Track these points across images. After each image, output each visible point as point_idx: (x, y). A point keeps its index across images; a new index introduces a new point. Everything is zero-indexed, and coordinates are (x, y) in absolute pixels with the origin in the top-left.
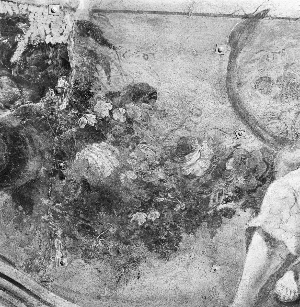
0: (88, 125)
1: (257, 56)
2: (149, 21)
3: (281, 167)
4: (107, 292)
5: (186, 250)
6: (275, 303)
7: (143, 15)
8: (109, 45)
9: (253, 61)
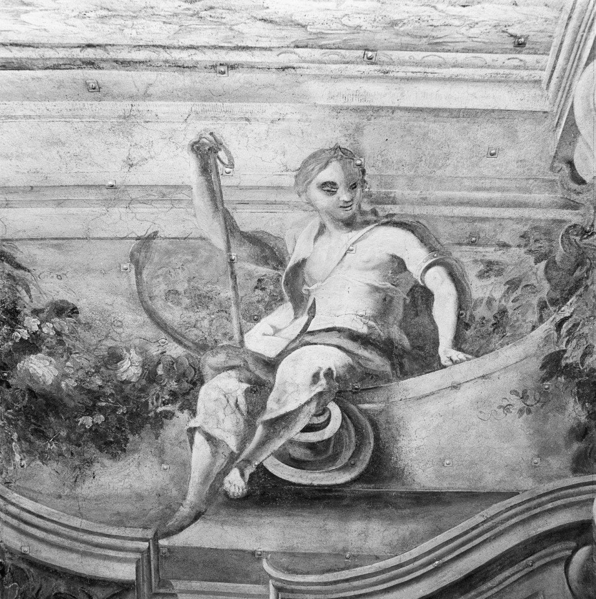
0: (22, 339)
1: (160, 272)
3: (207, 371)
4: (67, 491)
5: (135, 451)
6: (226, 499)
7: (47, 242)
8: (24, 269)
9: (158, 276)
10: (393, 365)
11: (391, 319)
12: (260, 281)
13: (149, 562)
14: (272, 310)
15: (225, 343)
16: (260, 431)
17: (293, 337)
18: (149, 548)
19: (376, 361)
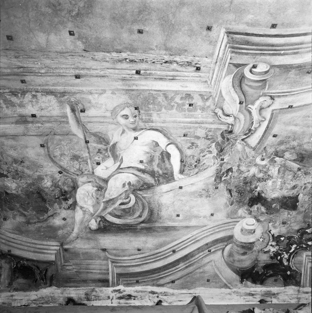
2: (11, 138)
3: (79, 183)
9: (56, 149)
10: (155, 180)
11: (154, 163)
12: (99, 150)
13: (60, 254)
14: (105, 160)
15: (86, 173)
16: (102, 205)
17: (114, 170)
18: (60, 249)
19: (148, 179)
